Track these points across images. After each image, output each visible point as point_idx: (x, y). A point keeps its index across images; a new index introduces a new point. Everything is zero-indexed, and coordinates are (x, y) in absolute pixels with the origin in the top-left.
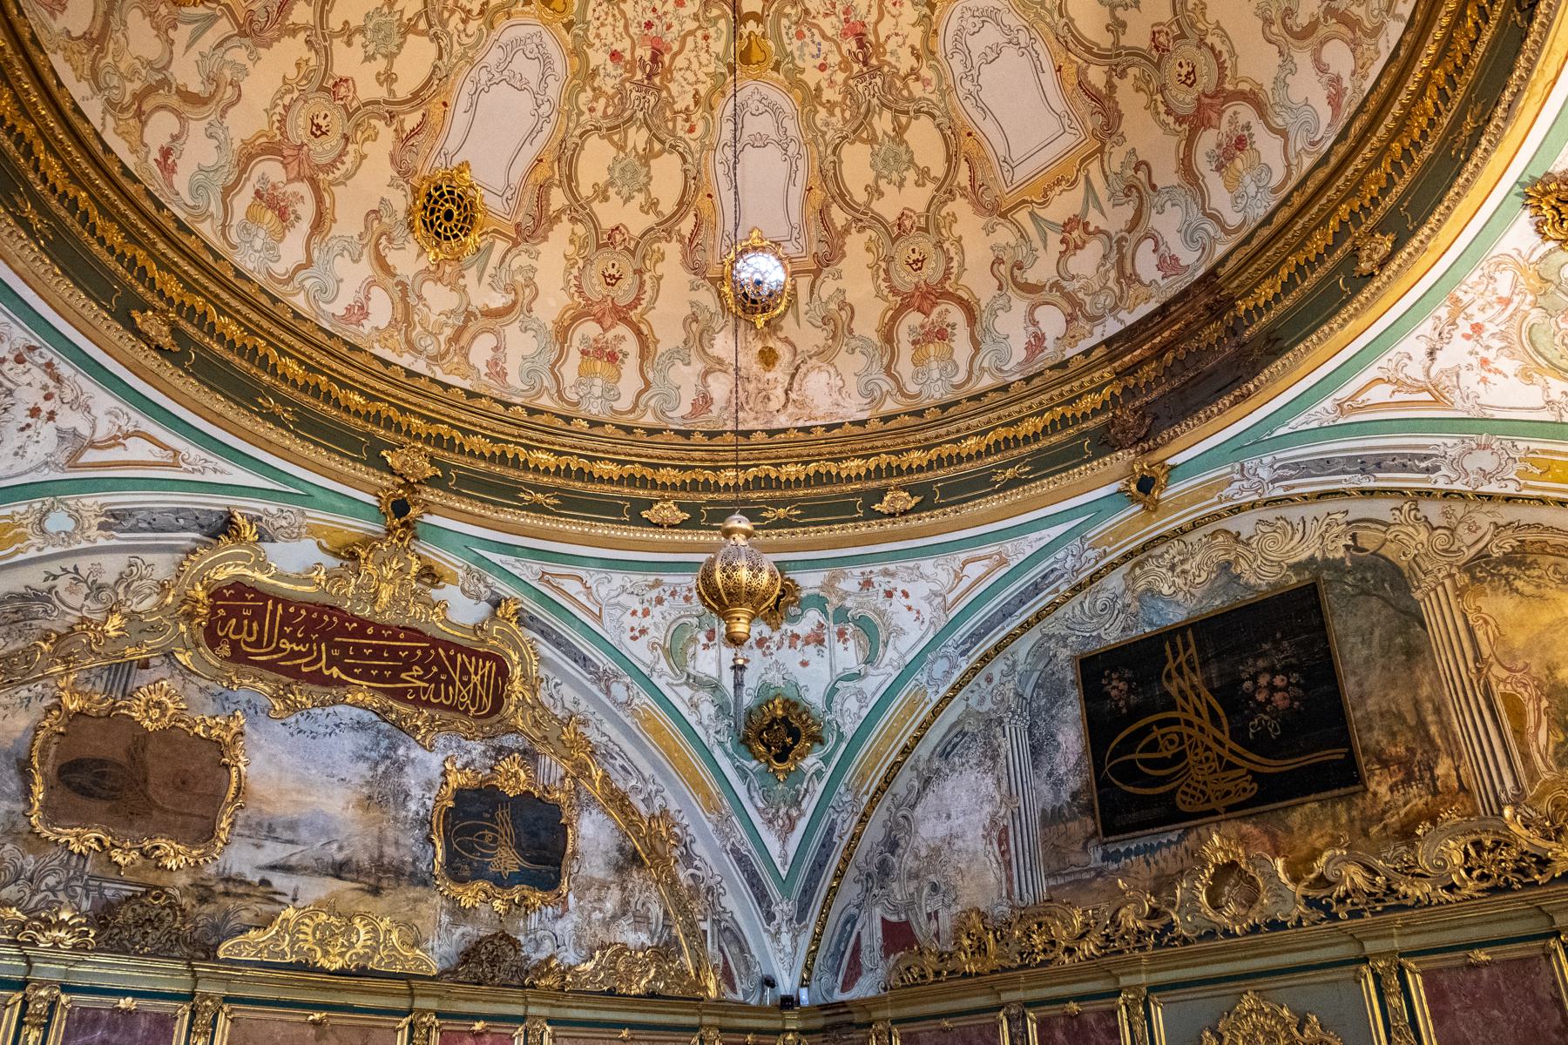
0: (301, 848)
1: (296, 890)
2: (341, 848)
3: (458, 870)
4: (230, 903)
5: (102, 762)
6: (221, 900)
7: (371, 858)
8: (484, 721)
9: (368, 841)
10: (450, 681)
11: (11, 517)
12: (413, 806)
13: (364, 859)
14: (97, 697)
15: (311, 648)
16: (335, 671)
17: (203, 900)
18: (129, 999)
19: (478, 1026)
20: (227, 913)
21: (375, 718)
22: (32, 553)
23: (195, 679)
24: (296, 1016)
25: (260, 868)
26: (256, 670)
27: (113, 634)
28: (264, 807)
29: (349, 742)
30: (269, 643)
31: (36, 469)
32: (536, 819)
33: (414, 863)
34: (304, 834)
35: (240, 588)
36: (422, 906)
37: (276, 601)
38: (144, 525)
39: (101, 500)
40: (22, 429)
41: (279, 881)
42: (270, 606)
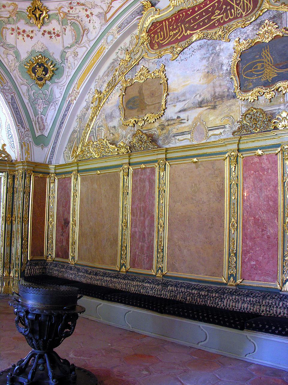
0: (187, 101)
1: (188, 117)
2: (200, 96)
3: (244, 88)
4: (170, 128)
5: (134, 98)
6: (167, 128)
7: (211, 96)
8: (250, 15)
9: (210, 89)
10: (232, 7)
11: (101, 45)
12: (225, 68)
13: (208, 97)
14: (129, 80)
15: (179, 29)
16: (189, 32)
17: (162, 129)
18: (143, 164)
19: (260, 152)
20: (169, 131)
21: (205, 41)
22: (107, 50)
23: (150, 61)
24: (188, 161)
25: (176, 113)
26: (165, 48)
27: (129, 60)
28: (175, 92)
29: (198, 55)
30: (167, 36)
31: (101, 29)
32: (284, 47)
33: (228, 90)
34: (188, 96)
35: (154, 24)
36: (234, 108)
37: (165, 20)
38: (126, 24)
39: (116, 26)
40: (90, 22)
41: (183, 115)
42: (164, 24)
